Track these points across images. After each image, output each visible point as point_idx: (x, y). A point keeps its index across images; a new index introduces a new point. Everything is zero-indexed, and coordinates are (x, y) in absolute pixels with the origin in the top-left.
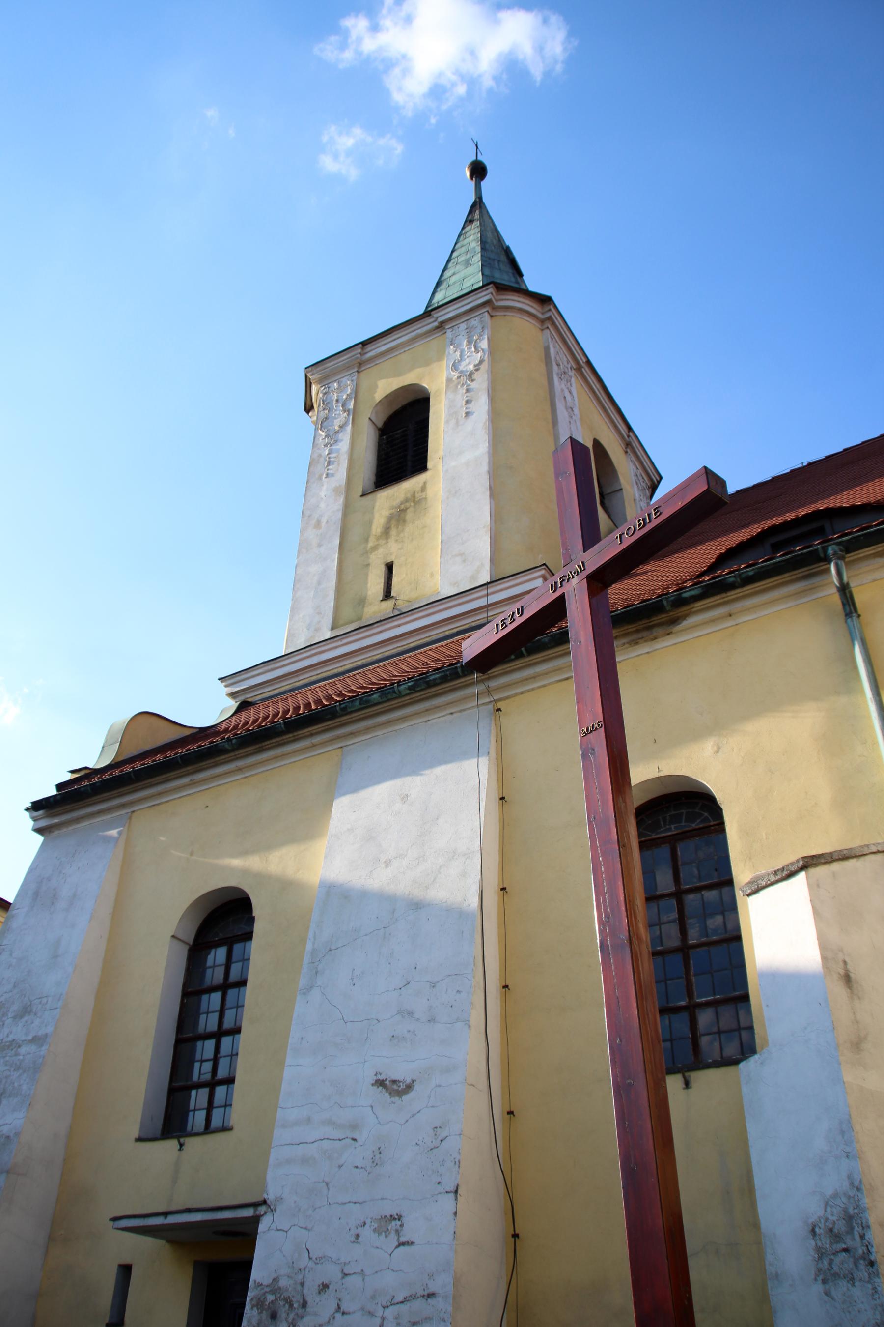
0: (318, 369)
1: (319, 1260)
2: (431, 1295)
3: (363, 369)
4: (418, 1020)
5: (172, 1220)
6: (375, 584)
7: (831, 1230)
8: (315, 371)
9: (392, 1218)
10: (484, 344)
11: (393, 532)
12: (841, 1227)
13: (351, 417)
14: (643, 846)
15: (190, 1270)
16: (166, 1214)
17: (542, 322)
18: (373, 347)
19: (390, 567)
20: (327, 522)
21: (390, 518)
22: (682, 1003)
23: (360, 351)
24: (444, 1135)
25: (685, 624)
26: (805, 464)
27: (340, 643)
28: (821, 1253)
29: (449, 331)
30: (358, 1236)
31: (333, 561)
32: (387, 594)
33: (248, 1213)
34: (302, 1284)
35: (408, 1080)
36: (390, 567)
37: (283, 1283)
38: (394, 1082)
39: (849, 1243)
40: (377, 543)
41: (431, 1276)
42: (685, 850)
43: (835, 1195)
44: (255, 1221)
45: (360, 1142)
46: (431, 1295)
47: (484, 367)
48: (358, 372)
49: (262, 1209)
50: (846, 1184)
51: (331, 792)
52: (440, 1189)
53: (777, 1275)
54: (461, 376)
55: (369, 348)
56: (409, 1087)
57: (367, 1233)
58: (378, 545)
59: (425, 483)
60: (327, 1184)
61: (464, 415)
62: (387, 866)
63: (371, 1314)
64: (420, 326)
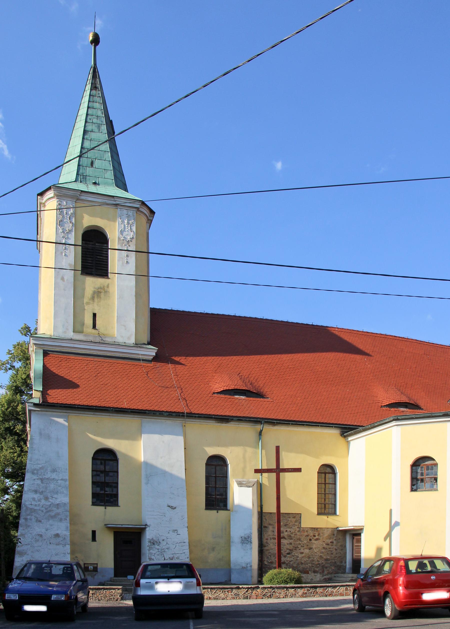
0: (58, 190)
1: (161, 536)
2: (184, 542)
3: (78, 202)
4: (175, 495)
5: (123, 526)
6: (89, 321)
7: (245, 538)
8: (56, 189)
9: (175, 530)
10: (134, 229)
11: (96, 300)
12: (247, 538)
13: (74, 228)
14: (36, 360)
15: (113, 533)
16: (122, 525)
17: (148, 220)
18: (85, 195)
19: (95, 315)
20: (67, 280)
21: (94, 293)
22: (214, 497)
23: (79, 194)
24: (184, 518)
25: (230, 423)
26: (205, 312)
27: (82, 344)
28: (242, 540)
29: (119, 210)
30: (169, 533)
31: (72, 301)
32: (94, 326)
33: (144, 527)
34: (159, 539)
35: (175, 507)
36: (95, 315)
37: (154, 539)
38: (172, 506)
39: (248, 540)
40: (89, 301)
41: (184, 540)
42: (218, 468)
43: (247, 534)
44: (145, 528)
45: (166, 516)
46: (184, 542)
47: (134, 241)
48: (75, 202)
49: (147, 526)
50: (249, 533)
51: (140, 432)
52: (184, 526)
53: (233, 542)
54: (124, 240)
55: (83, 194)
56: (175, 508)
57: (170, 532)
58: (89, 302)
59: (108, 284)
60: (161, 523)
61: (126, 262)
62: (161, 458)
63: (174, 544)
64: (108, 199)
